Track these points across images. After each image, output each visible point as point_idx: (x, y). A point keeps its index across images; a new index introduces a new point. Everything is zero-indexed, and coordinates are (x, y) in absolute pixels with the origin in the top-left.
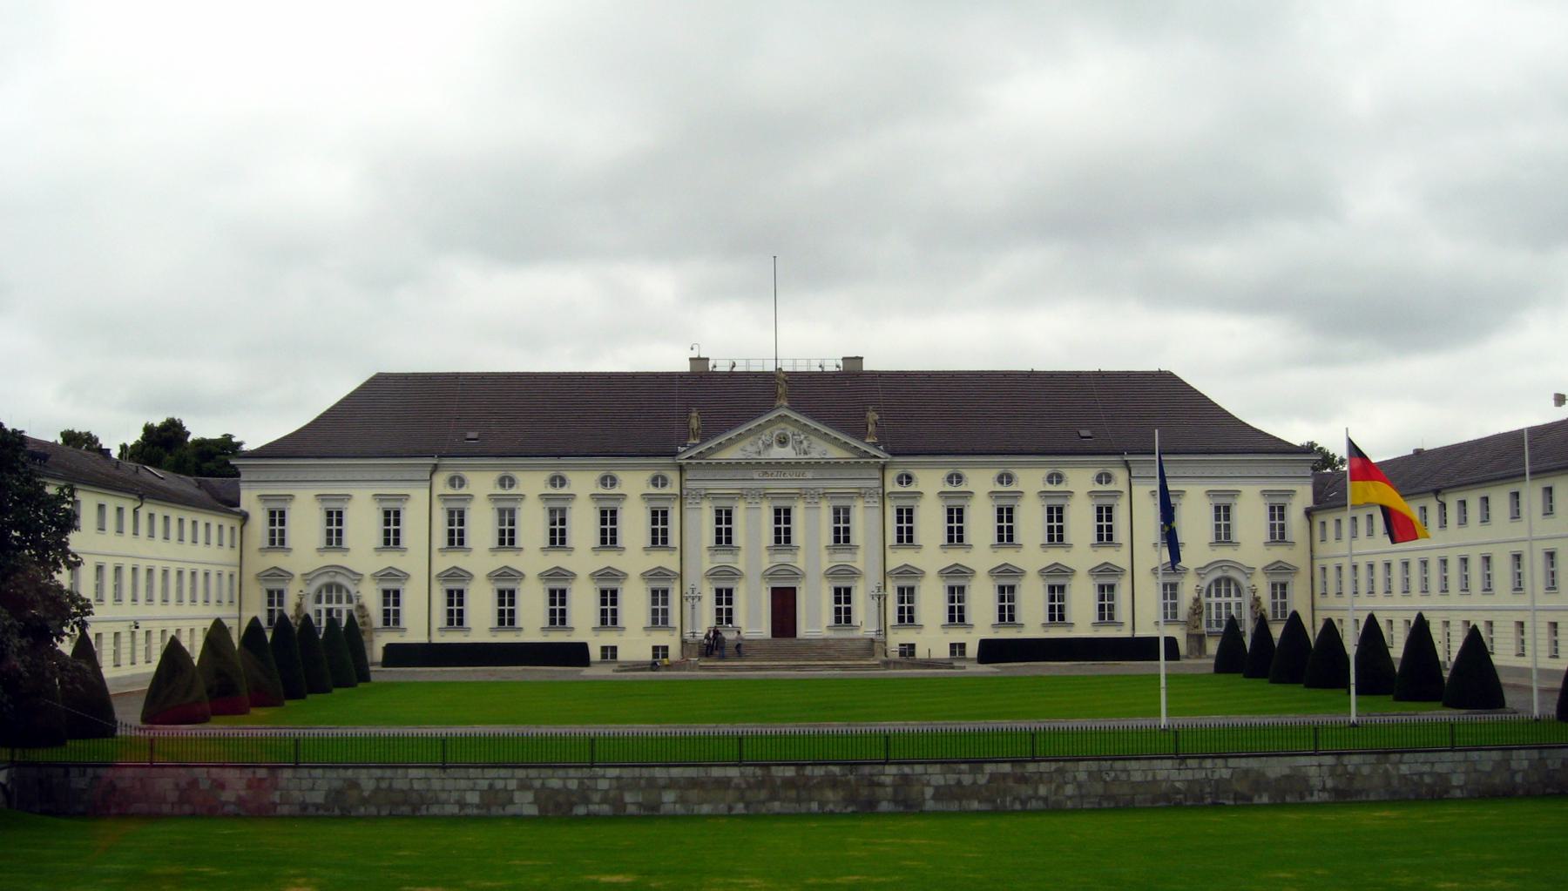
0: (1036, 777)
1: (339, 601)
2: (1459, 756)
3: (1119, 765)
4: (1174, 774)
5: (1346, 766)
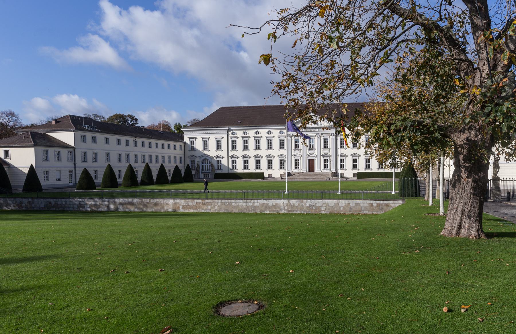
0: (208, 204)
1: (208, 163)
2: (324, 201)
3: (230, 201)
4: (244, 204)
5: (291, 203)
